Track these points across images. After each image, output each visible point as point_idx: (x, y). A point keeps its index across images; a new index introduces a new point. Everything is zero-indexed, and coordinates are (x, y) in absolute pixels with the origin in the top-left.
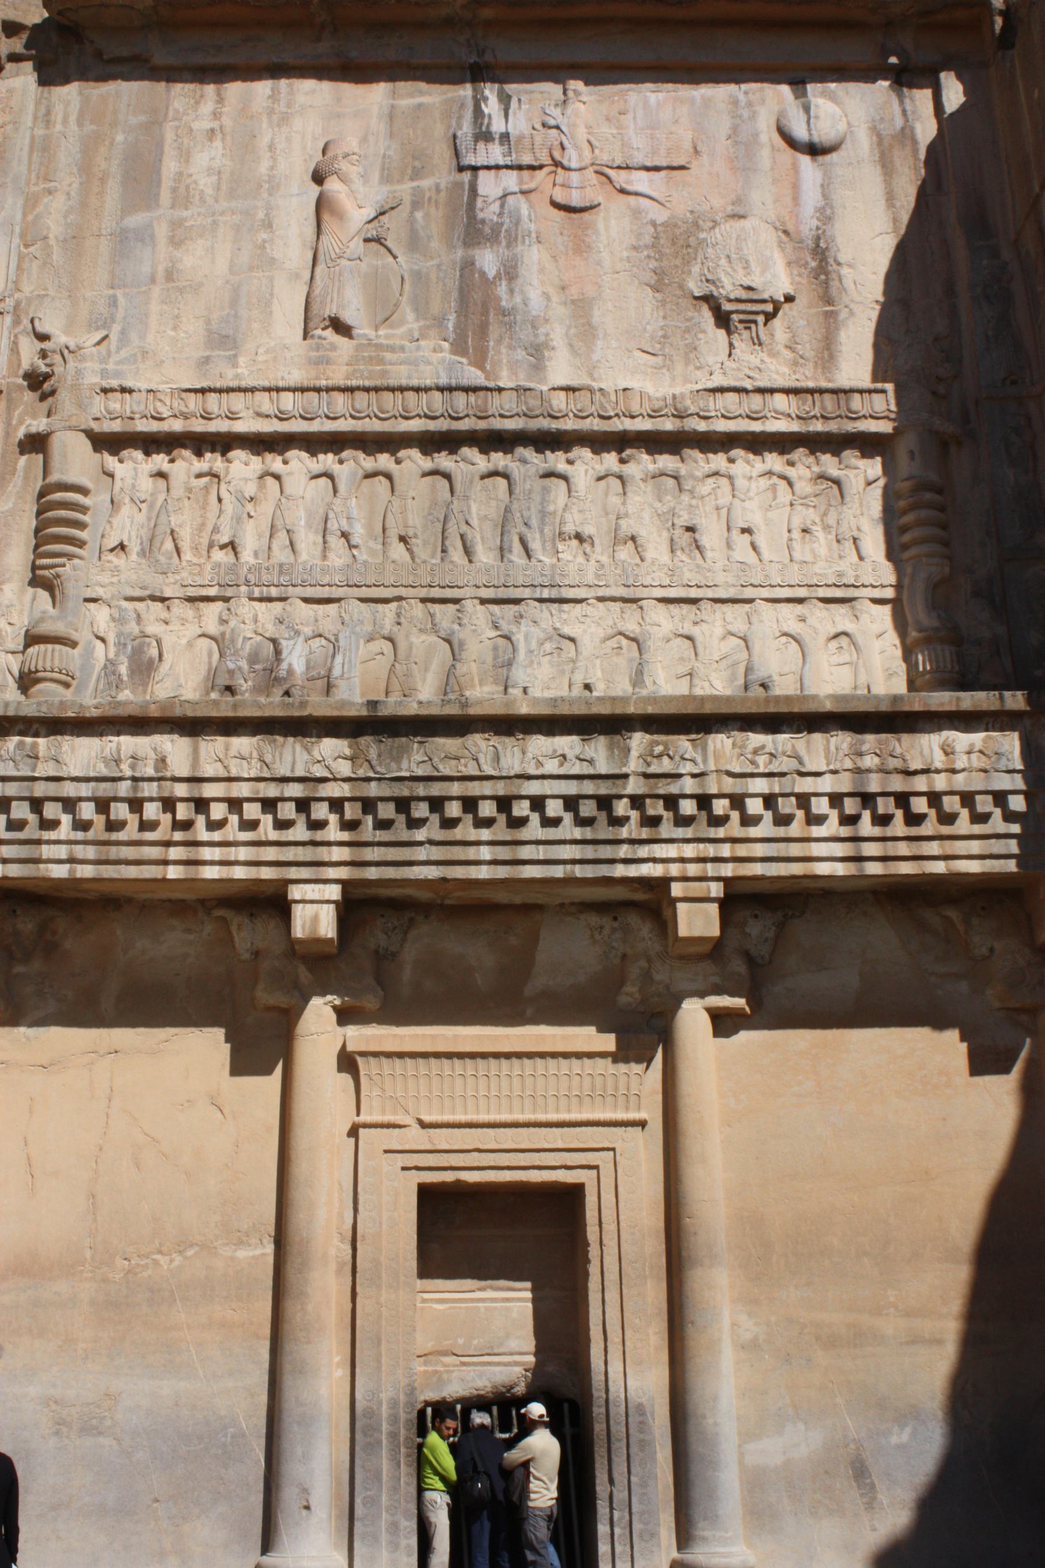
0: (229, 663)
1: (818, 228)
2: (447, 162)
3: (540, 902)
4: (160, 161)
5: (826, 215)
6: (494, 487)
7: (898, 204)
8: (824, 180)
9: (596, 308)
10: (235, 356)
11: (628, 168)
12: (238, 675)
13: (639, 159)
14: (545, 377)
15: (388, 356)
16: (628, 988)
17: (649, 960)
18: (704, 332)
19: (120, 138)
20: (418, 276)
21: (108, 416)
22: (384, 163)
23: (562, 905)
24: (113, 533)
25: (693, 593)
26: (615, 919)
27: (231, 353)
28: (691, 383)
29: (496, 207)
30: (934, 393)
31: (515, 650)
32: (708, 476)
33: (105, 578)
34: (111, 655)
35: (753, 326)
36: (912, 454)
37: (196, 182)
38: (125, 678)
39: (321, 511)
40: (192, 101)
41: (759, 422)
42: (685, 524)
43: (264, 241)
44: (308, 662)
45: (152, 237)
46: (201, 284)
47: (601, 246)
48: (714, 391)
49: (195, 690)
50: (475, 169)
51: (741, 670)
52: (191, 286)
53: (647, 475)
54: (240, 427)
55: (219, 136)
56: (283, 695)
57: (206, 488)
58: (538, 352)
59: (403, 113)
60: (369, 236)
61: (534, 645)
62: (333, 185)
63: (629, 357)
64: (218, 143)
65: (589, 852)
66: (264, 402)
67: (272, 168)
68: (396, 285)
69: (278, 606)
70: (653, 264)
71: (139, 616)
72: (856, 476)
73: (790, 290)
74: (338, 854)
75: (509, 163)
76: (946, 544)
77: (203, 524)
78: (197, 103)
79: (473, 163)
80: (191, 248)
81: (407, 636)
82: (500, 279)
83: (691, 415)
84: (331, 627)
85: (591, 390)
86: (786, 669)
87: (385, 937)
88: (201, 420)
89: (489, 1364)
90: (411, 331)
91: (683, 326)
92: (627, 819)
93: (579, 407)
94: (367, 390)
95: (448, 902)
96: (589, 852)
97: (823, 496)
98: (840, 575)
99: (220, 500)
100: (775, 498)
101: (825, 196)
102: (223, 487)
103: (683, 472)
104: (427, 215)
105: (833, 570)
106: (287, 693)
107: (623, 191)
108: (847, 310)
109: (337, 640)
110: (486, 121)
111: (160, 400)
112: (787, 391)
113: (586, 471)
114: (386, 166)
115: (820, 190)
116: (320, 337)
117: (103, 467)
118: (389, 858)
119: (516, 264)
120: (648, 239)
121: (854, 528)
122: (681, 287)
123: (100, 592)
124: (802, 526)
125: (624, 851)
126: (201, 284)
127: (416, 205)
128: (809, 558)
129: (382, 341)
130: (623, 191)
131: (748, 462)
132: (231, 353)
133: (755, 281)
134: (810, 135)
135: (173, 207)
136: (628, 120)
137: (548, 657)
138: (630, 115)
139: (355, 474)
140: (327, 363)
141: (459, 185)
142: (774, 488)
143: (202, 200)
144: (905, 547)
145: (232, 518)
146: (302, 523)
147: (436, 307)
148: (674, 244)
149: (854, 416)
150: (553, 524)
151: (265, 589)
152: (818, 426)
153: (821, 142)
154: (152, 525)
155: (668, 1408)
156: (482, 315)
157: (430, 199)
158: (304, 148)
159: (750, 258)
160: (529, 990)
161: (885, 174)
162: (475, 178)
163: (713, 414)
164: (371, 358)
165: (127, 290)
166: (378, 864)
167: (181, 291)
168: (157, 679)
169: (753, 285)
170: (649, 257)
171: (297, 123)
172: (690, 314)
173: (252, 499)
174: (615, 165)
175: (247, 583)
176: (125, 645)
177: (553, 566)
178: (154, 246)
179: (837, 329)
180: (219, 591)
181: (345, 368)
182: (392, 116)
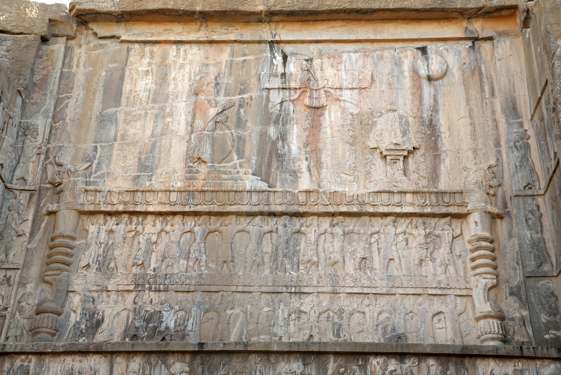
0: (136, 323)
1: (431, 115)
2: (256, 86)
4: (122, 85)
5: (435, 109)
6: (271, 238)
7: (472, 103)
8: (435, 93)
9: (323, 153)
10: (152, 175)
11: (341, 89)
12: (140, 329)
13: (345, 84)
14: (298, 186)
15: (223, 176)
18: (374, 165)
19: (104, 74)
20: (239, 138)
21: (87, 203)
22: (226, 86)
24: (85, 259)
25: (366, 291)
27: (150, 174)
28: (368, 189)
29: (278, 107)
30: (488, 194)
31: (278, 318)
32: (375, 233)
33: (79, 281)
34: (78, 319)
35: (398, 161)
36: (476, 222)
37: (139, 96)
38: (84, 331)
39: (187, 248)
40: (139, 58)
41: (399, 208)
42: (362, 257)
43: (169, 122)
44: (176, 322)
45: (116, 120)
46: (137, 142)
47: (327, 125)
48: (377, 192)
49: (118, 337)
50: (269, 89)
51: (389, 329)
52: (133, 142)
53: (344, 232)
54: (151, 209)
55: (151, 74)
56: (162, 340)
57: (134, 237)
58: (295, 174)
59: (237, 64)
60: (218, 120)
61: (286, 315)
62: (202, 97)
63: (337, 177)
64: (150, 77)
66: (162, 197)
67: (174, 89)
68: (229, 143)
69: (163, 296)
70: (351, 133)
71: (94, 300)
72: (448, 234)
73: (417, 145)
75: (285, 87)
76: (495, 268)
77: (130, 255)
78: (141, 58)
79: (268, 87)
80: (134, 125)
81: (225, 311)
82: (278, 141)
83: (366, 204)
84: (188, 306)
85: (318, 192)
86: (412, 330)
88: (133, 206)
90: (236, 164)
91: (364, 162)
93: (312, 200)
94: (212, 191)
97: (432, 243)
98: (439, 282)
99: (139, 243)
100: (407, 245)
101: (435, 100)
102: (141, 236)
103: (362, 231)
104: (245, 111)
105: (436, 280)
106: (164, 339)
107: (338, 99)
108: (445, 154)
109: (191, 312)
110: (275, 67)
111: (113, 196)
112: (413, 193)
113: (315, 231)
114: (228, 88)
115: (432, 97)
116: (192, 167)
117: (83, 227)
119: (286, 133)
120: (349, 122)
121: (446, 259)
122: (364, 143)
123: (76, 288)
124: (420, 258)
126: (137, 142)
127: (241, 106)
128: (424, 274)
129: (222, 169)
130: (338, 99)
131: (394, 226)
132: (150, 174)
133: (399, 140)
134: (429, 72)
135: (127, 106)
136: (342, 67)
137: (293, 322)
138: (343, 65)
139: (205, 231)
140: (194, 179)
141: (261, 97)
142: (407, 240)
143: (141, 103)
144: (473, 268)
145: (144, 252)
146: (178, 254)
147: (247, 153)
148: (361, 123)
149: (447, 205)
150: (298, 256)
151: (157, 286)
152: (428, 210)
153: (433, 75)
154: (105, 255)
156: (269, 157)
157: (247, 103)
158: (190, 79)
159: (396, 130)
161: (465, 89)
162: (269, 93)
163: (377, 203)
164: (215, 177)
165: (102, 144)
167: (128, 144)
168: (100, 331)
169: (398, 142)
170: (349, 130)
171: (187, 69)
172: (368, 156)
173: (155, 243)
174: (335, 87)
175: (149, 283)
176: (86, 314)
177: (298, 277)
178: (117, 124)
179: (440, 163)
180: (135, 287)
181: (202, 181)
182: (231, 65)
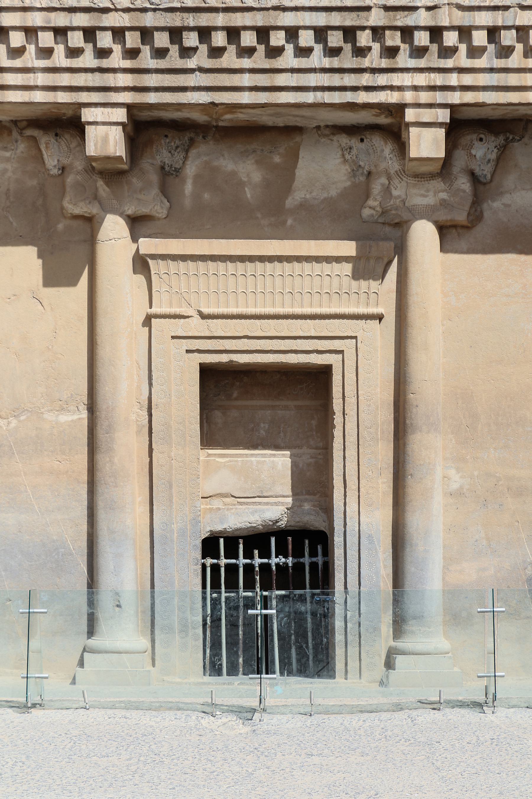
3: (299, 124)
16: (371, 202)
17: (389, 178)
23: (318, 128)
26: (362, 140)
65: (336, 80)
74: (124, 80)
87: (170, 155)
89: (260, 503)
92: (369, 49)
95: (221, 124)
96: (336, 80)
118: (166, 84)
125: (366, 79)
155: (390, 538)
160: (290, 203)
166: (157, 89)
